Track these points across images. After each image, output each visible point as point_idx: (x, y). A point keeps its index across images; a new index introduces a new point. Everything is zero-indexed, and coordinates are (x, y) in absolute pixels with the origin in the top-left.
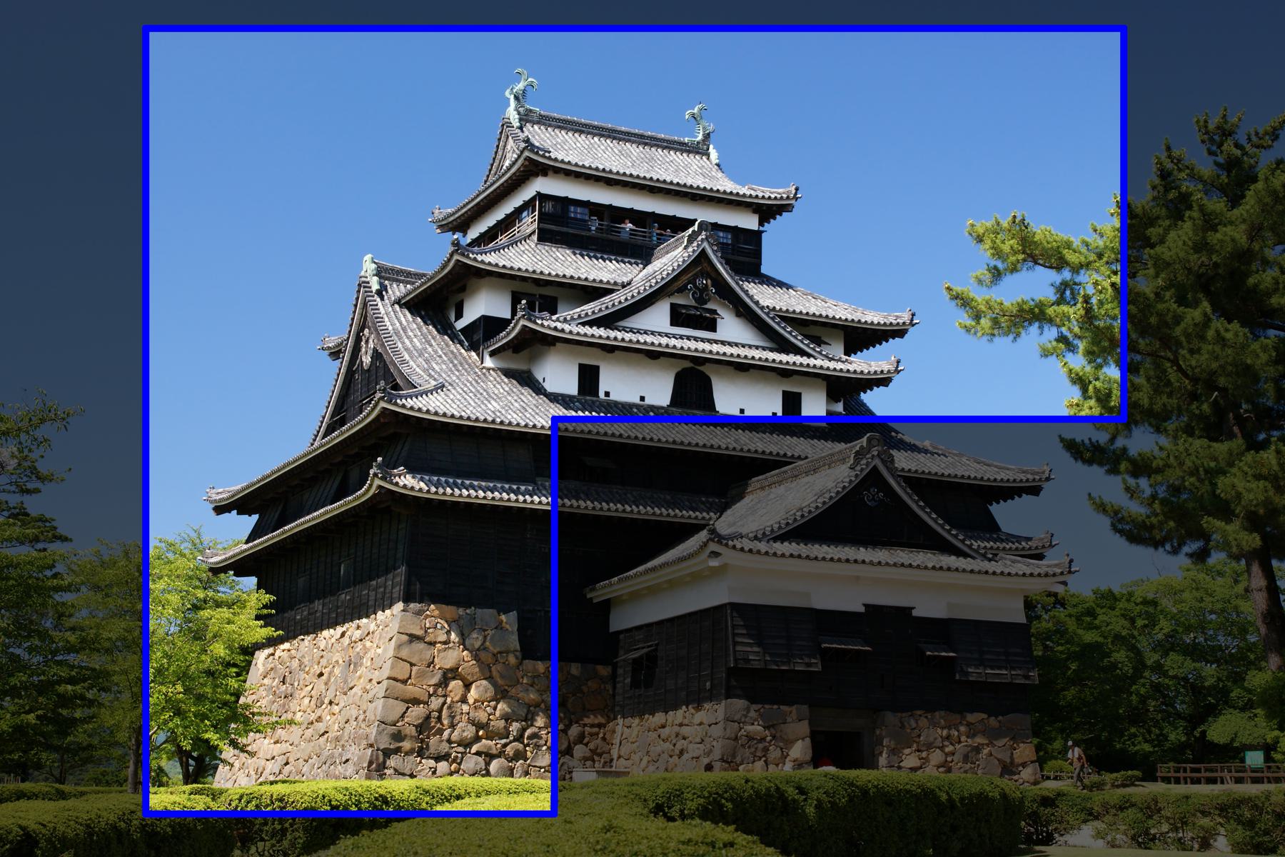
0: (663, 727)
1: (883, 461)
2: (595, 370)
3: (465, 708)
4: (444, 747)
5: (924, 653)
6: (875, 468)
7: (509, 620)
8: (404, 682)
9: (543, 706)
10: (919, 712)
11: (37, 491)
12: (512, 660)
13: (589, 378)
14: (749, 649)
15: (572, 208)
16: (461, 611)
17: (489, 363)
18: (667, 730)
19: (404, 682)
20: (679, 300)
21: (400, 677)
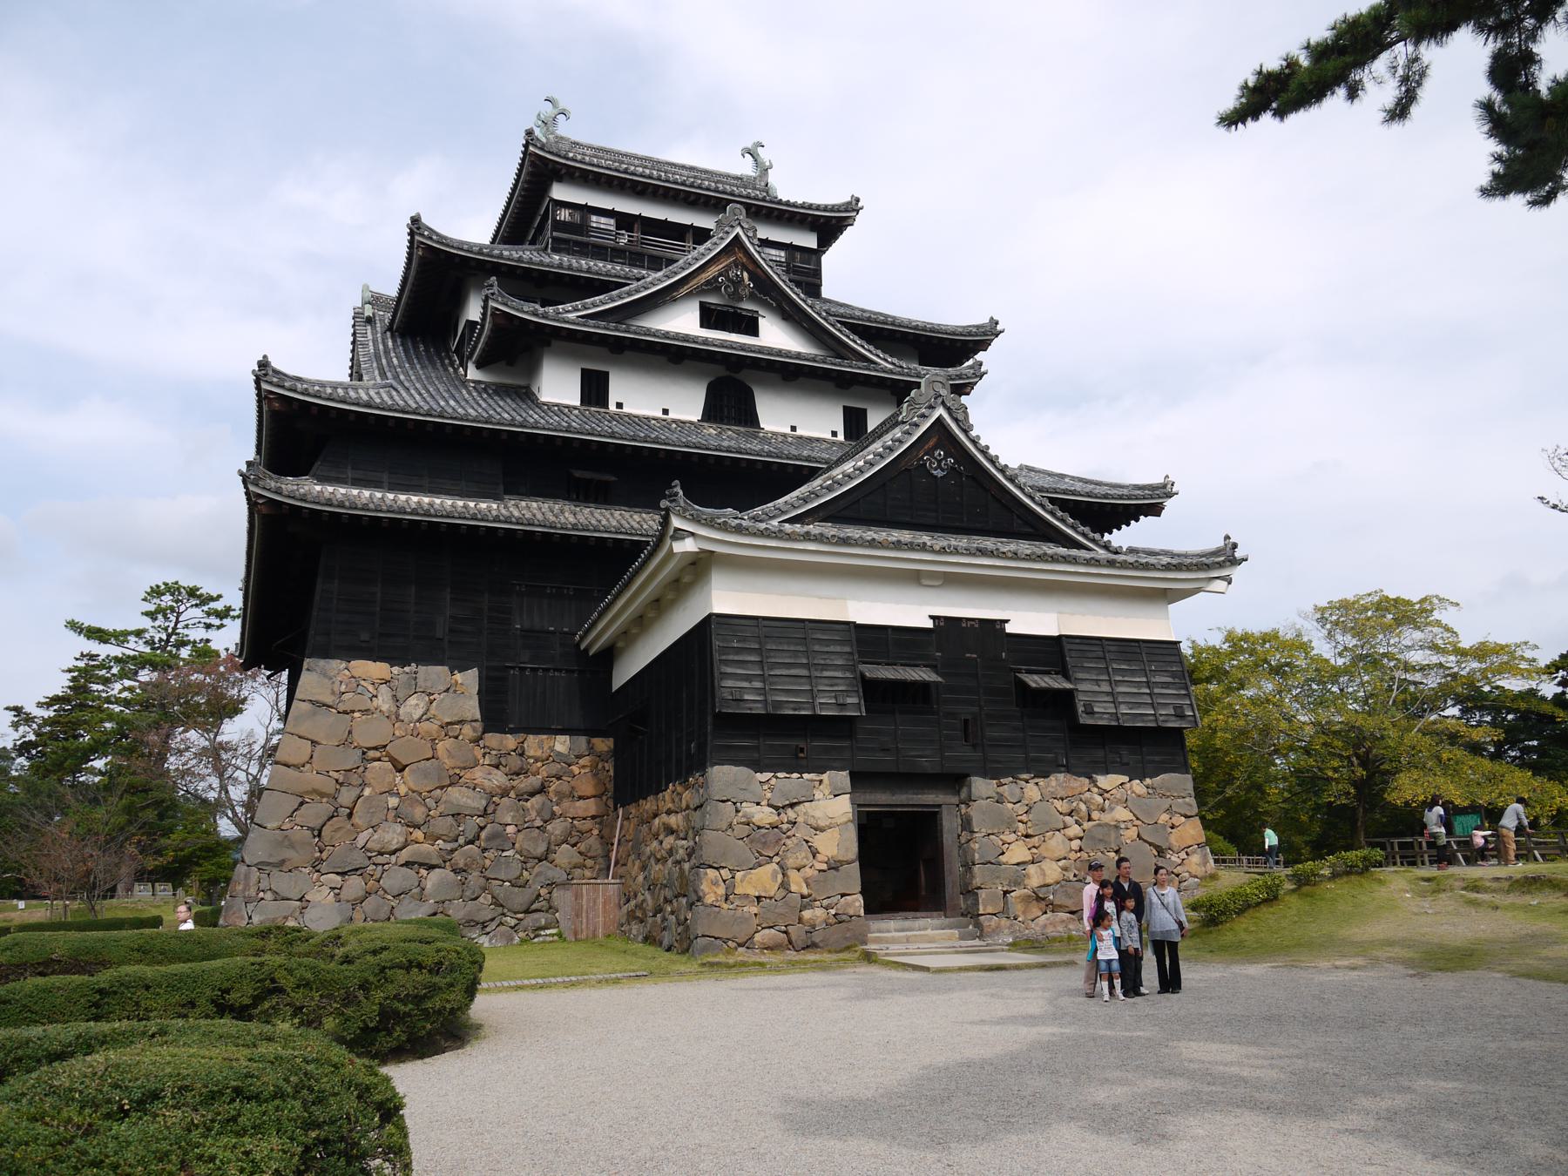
0: (656, 816)
1: (948, 409)
2: (604, 378)
3: (393, 802)
4: (359, 859)
5: (1025, 685)
6: (939, 420)
7: (469, 679)
8: (296, 767)
9: (512, 794)
10: (1025, 776)
11: (222, 626)
12: (468, 731)
13: (594, 389)
14: (745, 684)
15: (594, 218)
16: (396, 670)
17: (473, 373)
18: (657, 821)
19: (296, 767)
20: (712, 300)
21: (291, 761)
